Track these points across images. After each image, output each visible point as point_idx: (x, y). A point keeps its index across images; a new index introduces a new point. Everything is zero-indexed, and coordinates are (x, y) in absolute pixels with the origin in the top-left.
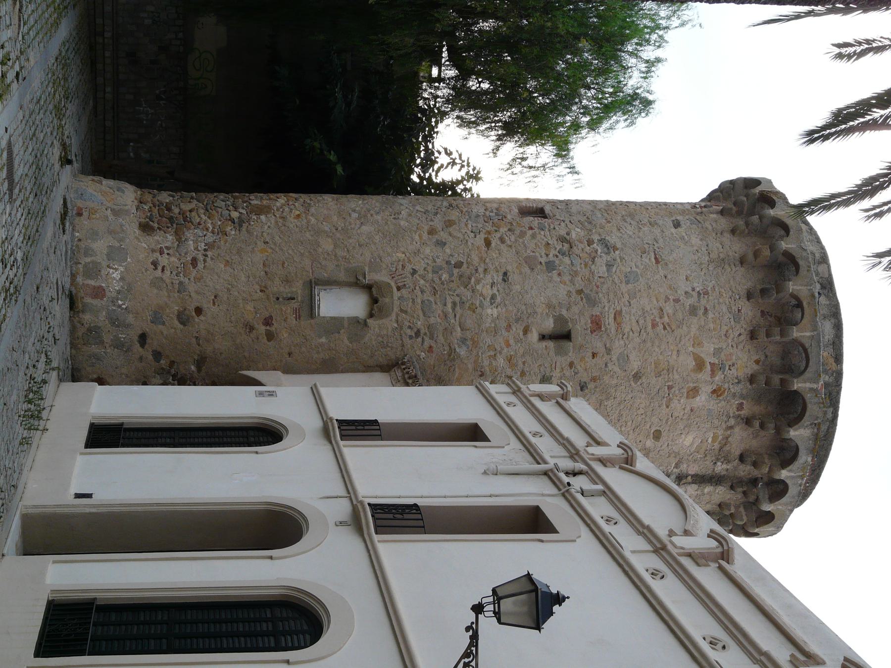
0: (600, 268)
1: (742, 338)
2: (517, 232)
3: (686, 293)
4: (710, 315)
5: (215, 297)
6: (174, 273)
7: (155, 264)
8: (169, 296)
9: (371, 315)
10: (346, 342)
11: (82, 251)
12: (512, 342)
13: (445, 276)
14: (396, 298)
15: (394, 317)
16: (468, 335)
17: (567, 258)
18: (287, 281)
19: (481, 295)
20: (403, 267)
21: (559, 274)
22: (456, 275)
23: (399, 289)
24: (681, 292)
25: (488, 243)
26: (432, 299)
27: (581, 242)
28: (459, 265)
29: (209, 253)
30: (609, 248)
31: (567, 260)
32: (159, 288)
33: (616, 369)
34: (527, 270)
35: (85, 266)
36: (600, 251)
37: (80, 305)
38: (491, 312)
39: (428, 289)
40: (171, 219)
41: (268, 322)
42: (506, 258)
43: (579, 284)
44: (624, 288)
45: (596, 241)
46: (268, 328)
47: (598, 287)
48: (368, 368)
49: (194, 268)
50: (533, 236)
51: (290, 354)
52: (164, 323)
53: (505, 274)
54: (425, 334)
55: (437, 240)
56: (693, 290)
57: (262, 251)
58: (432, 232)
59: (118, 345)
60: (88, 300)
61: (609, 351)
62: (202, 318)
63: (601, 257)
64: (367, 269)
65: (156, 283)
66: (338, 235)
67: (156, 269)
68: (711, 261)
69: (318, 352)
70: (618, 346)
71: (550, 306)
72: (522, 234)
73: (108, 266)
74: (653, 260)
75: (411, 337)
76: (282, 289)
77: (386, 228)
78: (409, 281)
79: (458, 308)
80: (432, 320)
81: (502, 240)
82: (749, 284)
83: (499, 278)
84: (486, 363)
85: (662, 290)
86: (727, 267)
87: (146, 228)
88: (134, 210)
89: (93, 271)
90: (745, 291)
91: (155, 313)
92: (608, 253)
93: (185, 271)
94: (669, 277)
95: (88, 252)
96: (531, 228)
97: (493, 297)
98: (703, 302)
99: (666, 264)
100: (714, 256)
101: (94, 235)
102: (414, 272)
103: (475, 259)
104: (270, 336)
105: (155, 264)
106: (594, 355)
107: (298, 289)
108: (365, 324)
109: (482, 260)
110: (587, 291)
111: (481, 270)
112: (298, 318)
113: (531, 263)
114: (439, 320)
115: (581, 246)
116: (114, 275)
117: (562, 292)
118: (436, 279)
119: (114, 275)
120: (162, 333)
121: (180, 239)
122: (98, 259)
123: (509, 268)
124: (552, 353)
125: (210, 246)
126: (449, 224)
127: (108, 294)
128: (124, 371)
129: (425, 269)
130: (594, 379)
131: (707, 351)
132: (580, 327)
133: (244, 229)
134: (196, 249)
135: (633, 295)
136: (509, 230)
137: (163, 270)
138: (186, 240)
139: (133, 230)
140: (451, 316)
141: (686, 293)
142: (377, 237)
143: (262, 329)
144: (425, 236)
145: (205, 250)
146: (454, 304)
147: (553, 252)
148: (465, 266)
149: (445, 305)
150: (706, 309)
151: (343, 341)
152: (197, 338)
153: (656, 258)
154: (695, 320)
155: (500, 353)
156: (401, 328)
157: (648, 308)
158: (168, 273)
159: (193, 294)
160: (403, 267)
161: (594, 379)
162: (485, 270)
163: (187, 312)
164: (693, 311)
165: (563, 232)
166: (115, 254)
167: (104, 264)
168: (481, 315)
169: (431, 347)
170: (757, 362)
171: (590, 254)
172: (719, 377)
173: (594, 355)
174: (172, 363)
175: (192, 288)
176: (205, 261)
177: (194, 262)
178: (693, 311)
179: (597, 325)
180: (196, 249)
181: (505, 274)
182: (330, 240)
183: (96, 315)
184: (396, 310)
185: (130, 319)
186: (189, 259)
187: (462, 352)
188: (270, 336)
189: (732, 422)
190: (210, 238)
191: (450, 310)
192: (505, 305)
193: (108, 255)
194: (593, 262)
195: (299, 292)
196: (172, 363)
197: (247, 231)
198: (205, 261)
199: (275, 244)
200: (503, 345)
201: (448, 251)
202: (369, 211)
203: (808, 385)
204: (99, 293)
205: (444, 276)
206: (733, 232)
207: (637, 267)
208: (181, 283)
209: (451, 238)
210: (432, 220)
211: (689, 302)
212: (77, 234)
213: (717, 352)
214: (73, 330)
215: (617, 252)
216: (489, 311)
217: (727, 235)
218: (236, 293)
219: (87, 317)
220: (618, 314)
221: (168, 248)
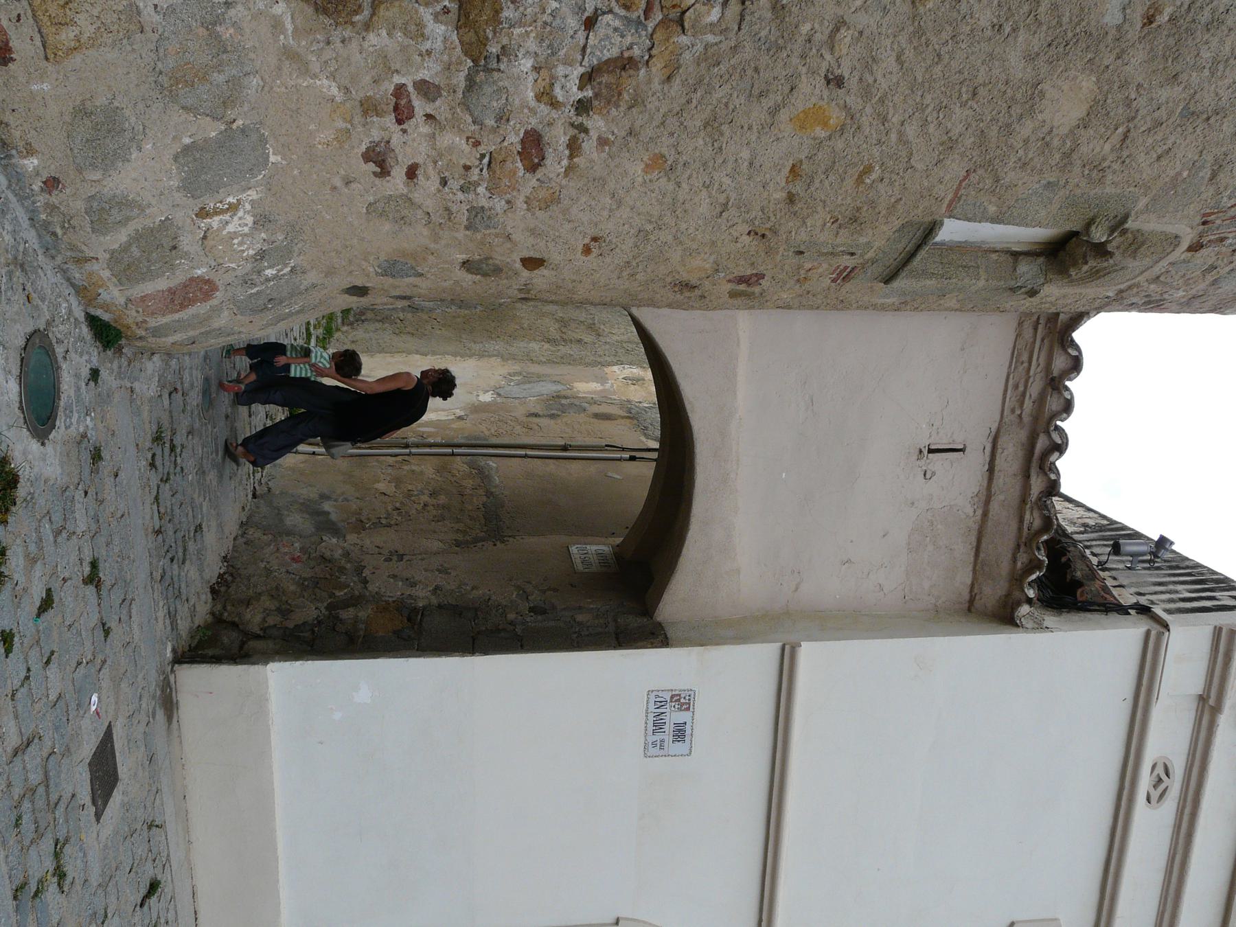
29: (596, 123)
49: (533, 168)
67: (384, 171)
73: (203, 213)
101: (102, 133)
105: (379, 159)
125: (609, 79)
134: (546, 96)
137: (412, 173)
145: (583, 107)
158: (428, 183)
167: (183, 215)
176: (574, 147)
185: (312, 277)
186: (514, 139)
193: (190, 187)
198: (574, 147)
199: (866, 93)
208: (476, 212)
212: (31, 163)
221: (427, 89)
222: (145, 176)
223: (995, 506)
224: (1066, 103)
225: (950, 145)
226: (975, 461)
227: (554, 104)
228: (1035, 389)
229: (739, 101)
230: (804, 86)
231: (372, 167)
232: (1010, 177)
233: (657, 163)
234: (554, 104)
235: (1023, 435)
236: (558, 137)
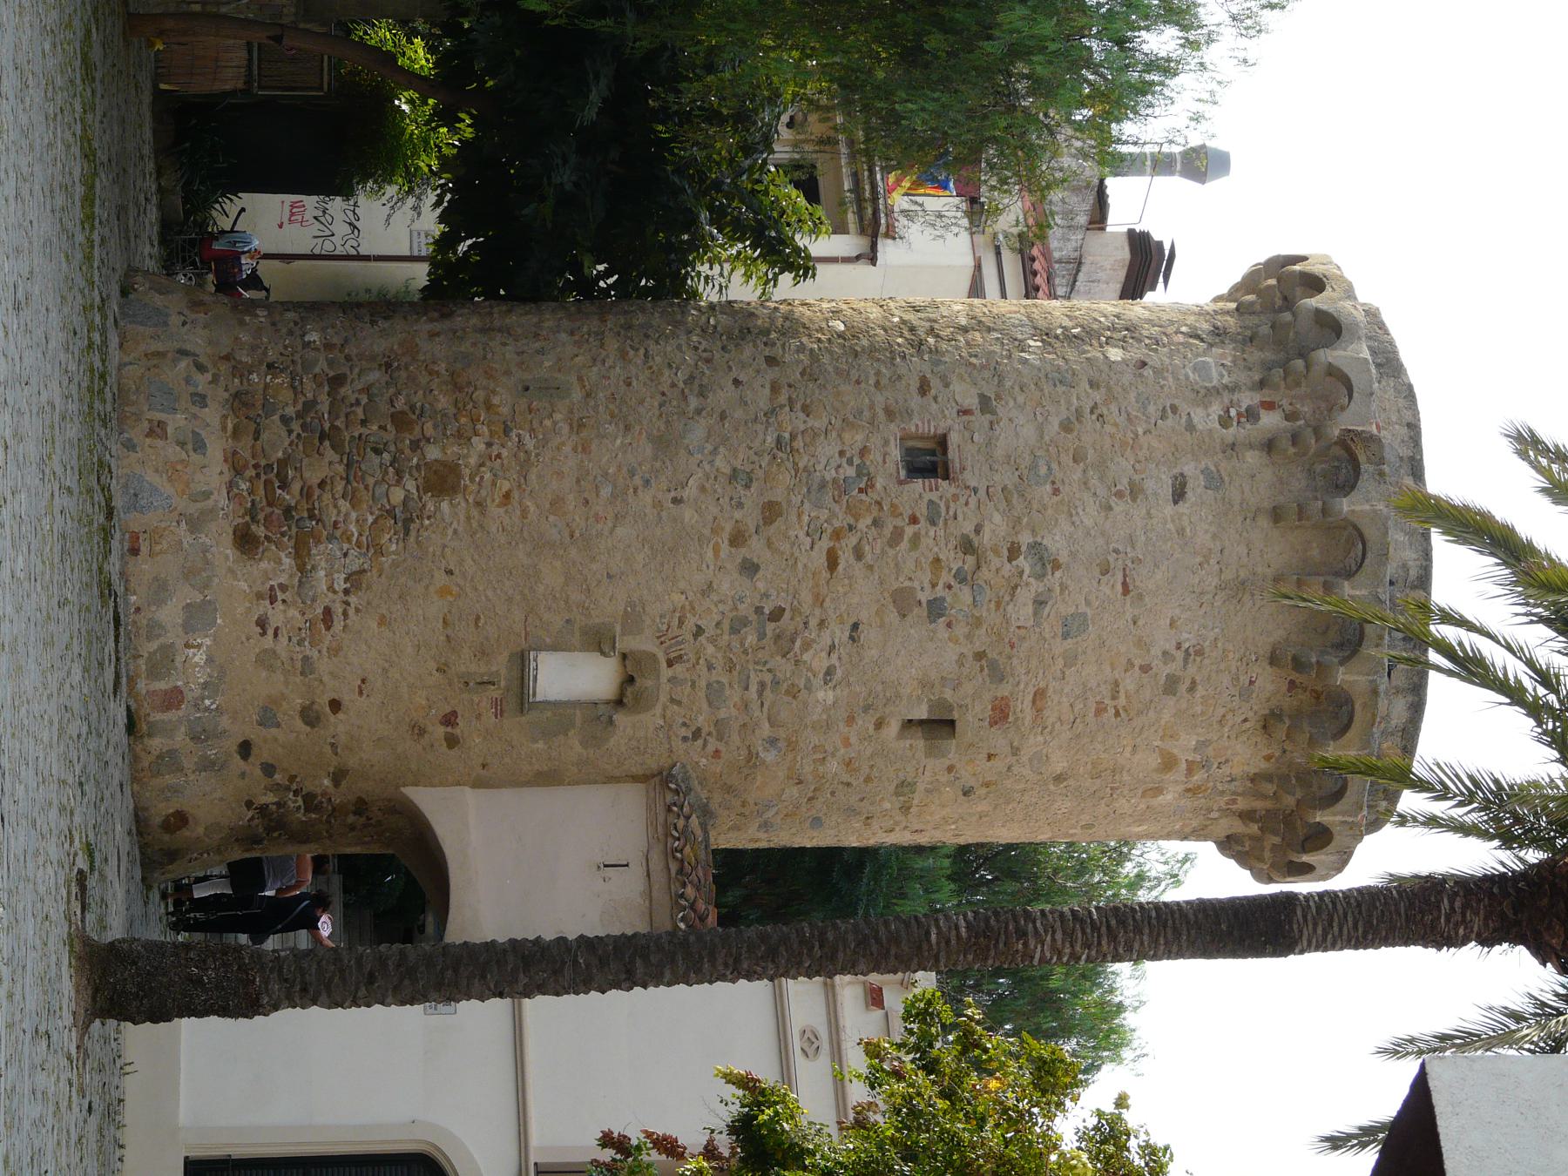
0: (1022, 611)
1: (1248, 725)
2: (887, 531)
3: (1165, 653)
4: (1200, 691)
5: (363, 681)
6: (295, 640)
7: (262, 623)
8: (287, 683)
9: (619, 702)
10: (578, 748)
11: (143, 632)
12: (853, 740)
13: (751, 639)
14: (664, 680)
15: (658, 710)
16: (782, 733)
17: (966, 590)
18: (483, 653)
19: (810, 669)
20: (681, 623)
21: (949, 625)
22: (769, 633)
23: (670, 664)
24: (1156, 651)
25: (832, 562)
26: (725, 680)
27: (996, 552)
28: (777, 614)
29: (353, 599)
30: (1045, 562)
31: (965, 595)
32: (271, 668)
33: (1026, 772)
34: (892, 616)
35: (149, 659)
36: (1027, 571)
37: (145, 727)
38: (825, 695)
39: (719, 663)
40: (288, 511)
41: (449, 720)
42: (860, 592)
43: (981, 641)
44: (1060, 646)
45: (1024, 548)
46: (449, 729)
47: (1012, 647)
48: (611, 779)
49: (328, 628)
50: (915, 540)
51: (484, 766)
52: (278, 725)
53: (855, 626)
54: (709, 734)
55: (745, 560)
56: (1179, 646)
57: (444, 592)
58: (737, 539)
59: (207, 765)
60: (157, 717)
61: (1015, 751)
62: (341, 715)
63: (1027, 584)
64: (618, 629)
65: (266, 660)
66: (573, 552)
67: (264, 634)
68: (1220, 588)
69: (531, 764)
70: (1034, 742)
71: (925, 684)
72: (897, 535)
73: (187, 646)
74: (1119, 588)
75: (685, 739)
76: (473, 668)
77: (658, 532)
78: (688, 649)
79: (767, 692)
80: (722, 714)
81: (859, 555)
82: (1279, 634)
83: (841, 634)
84: (808, 769)
85: (1123, 649)
86: (1247, 597)
87: (245, 541)
88: (223, 502)
89: (163, 662)
90: (1269, 648)
91: (265, 709)
92: (1040, 577)
93: (312, 636)
94: (1140, 623)
95: (154, 629)
96: (914, 520)
97: (829, 672)
98: (1192, 669)
99: (1140, 597)
100: (1228, 575)
101: (161, 590)
102: (699, 631)
103: (806, 597)
104: (452, 741)
105: (262, 623)
106: (990, 757)
107: (500, 665)
108: (611, 721)
109: (819, 601)
110: (992, 655)
111: (813, 622)
112: (499, 713)
113: (902, 601)
114: (734, 712)
115: (996, 562)
116: (196, 659)
117: (951, 654)
118: (736, 644)
119: (196, 659)
120: (276, 740)
121: (303, 569)
122: (169, 638)
123: (864, 616)
124: (920, 754)
125: (355, 580)
126: (771, 512)
127: (189, 696)
128: (218, 794)
129: (718, 624)
130: (987, 785)
131: (1185, 746)
132: (971, 720)
133: (412, 539)
134: (331, 588)
135: (1071, 660)
136: (875, 523)
137: (276, 635)
138: (313, 567)
139: (225, 551)
140: (755, 706)
141: (1165, 653)
143: (441, 730)
144: (725, 546)
145: (346, 592)
146: (762, 685)
147: (946, 577)
148: (787, 615)
149: (747, 688)
150: (1194, 682)
151: (572, 747)
152: (332, 745)
153: (1125, 584)
154: (1170, 701)
155: (833, 755)
156: (671, 726)
157: (1093, 683)
158: (283, 640)
159: (326, 679)
160: (681, 623)
161: (987, 785)
162: (822, 624)
163: (316, 707)
164: (1171, 686)
165: (968, 528)
166: (198, 616)
167: (179, 643)
168: (806, 705)
169: (717, 751)
170: (1268, 758)
171: (1008, 580)
172: (1198, 777)
173: (990, 757)
174: (292, 778)
175: (324, 666)
176: (345, 614)
177: (328, 612)
178: (1171, 686)
179: (1001, 714)
180: (331, 588)
181: (855, 626)
182: (558, 564)
183: (171, 734)
184: (663, 698)
185: (225, 722)
186: (320, 611)
187: (770, 757)
188: (452, 741)
189: (1214, 815)
190: (354, 563)
191: (755, 696)
192: (849, 684)
194: (1013, 595)
195: (503, 672)
196: (292, 778)
197: (418, 542)
198: (345, 614)
200: (839, 743)
201: (761, 585)
202: (632, 473)
203: (1339, 818)
204: (173, 699)
205: (750, 638)
206: (1276, 515)
207: (1088, 603)
208: (306, 659)
209: (768, 554)
210: (740, 505)
211: (1163, 671)
212: (133, 598)
213: (1201, 745)
214: (136, 759)
215: (1058, 574)
216: (821, 695)
217: (1264, 522)
218: (397, 676)
219: (157, 744)
220: (1039, 695)
221: (283, 588)
222: (170, 614)
223: (655, 894)
225: (510, 600)
226: (636, 872)
227: (335, 592)
228: (661, 819)
229: (410, 583)
230: (436, 574)
231: (258, 630)
232: (546, 616)
233: (382, 621)
234: (335, 592)
235: (661, 846)
236: (338, 609)
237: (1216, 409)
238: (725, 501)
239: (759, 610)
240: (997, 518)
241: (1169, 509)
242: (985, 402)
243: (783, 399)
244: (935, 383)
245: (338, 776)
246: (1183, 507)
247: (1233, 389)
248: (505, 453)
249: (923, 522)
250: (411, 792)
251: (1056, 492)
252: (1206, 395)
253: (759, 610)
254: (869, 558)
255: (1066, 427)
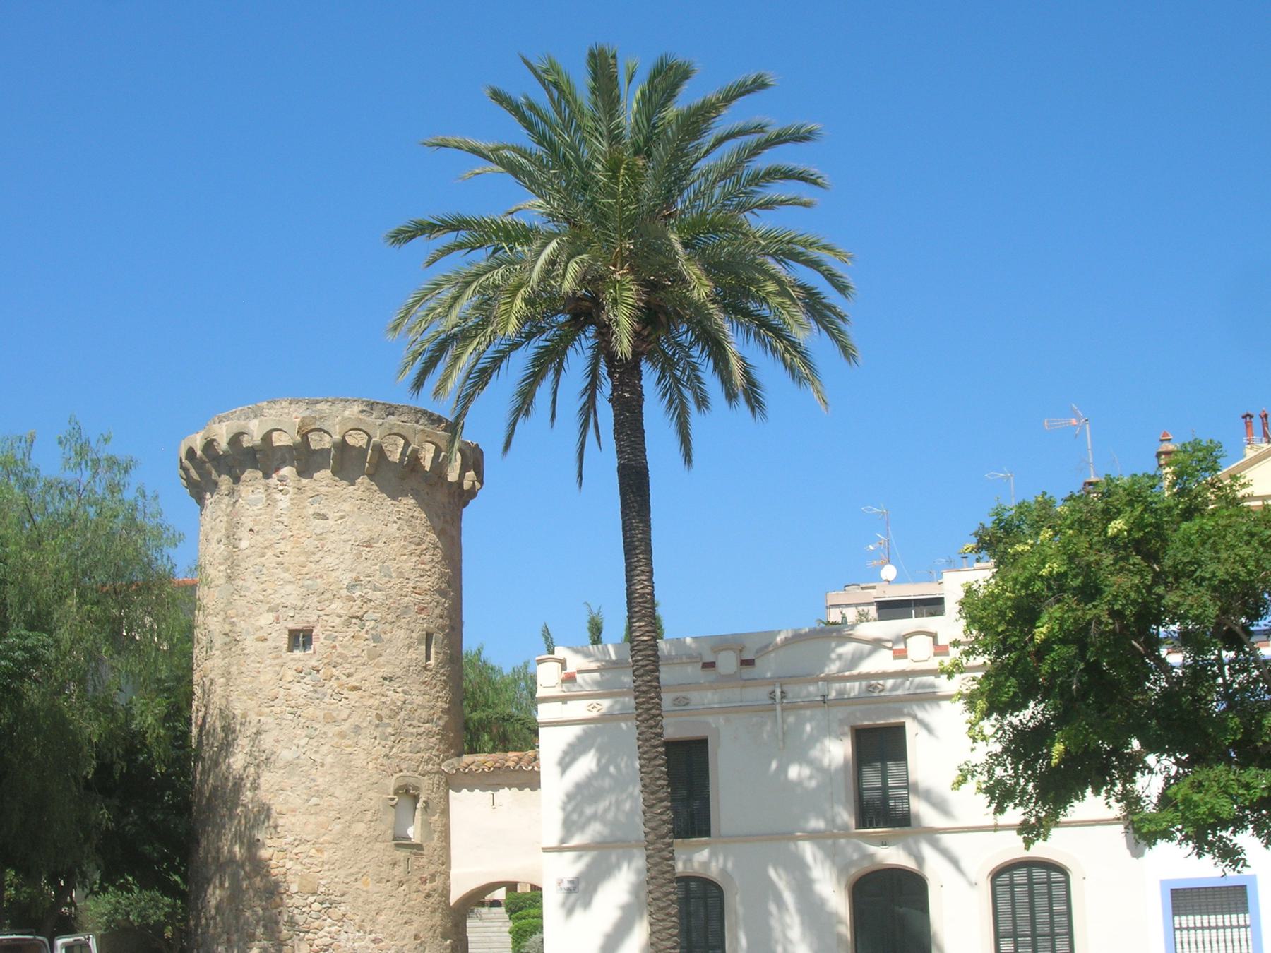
24: (398, 534)
25: (355, 689)
28: (380, 717)
53: (385, 679)
76: (401, 869)
96: (334, 647)
107: (401, 854)
111: (384, 699)
142: (351, 784)
177: (374, 941)
181: (385, 679)
197: (342, 895)
201: (365, 725)
224: (359, 828)
225: (370, 850)
236: (373, 936)
237: (279, 496)
238: (323, 741)
239: (377, 726)
240: (333, 606)
241: (331, 522)
242: (270, 610)
243: (268, 710)
244: (261, 634)
245: (445, 937)
246: (330, 515)
247: (268, 487)
248: (295, 851)
249: (336, 643)
250: (453, 901)
251: (321, 577)
252: (271, 502)
253: (377, 726)
254: (353, 670)
255: (287, 570)
